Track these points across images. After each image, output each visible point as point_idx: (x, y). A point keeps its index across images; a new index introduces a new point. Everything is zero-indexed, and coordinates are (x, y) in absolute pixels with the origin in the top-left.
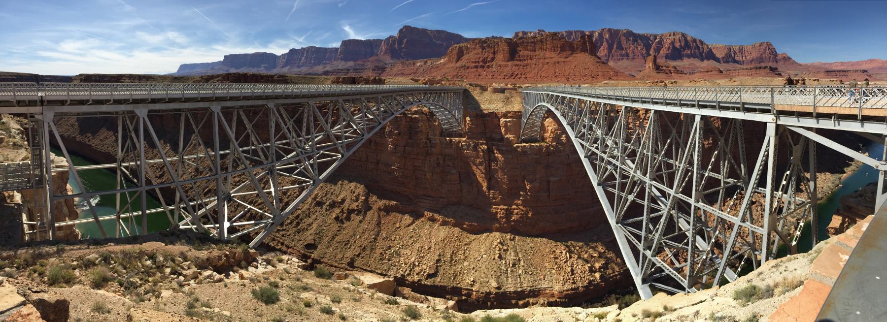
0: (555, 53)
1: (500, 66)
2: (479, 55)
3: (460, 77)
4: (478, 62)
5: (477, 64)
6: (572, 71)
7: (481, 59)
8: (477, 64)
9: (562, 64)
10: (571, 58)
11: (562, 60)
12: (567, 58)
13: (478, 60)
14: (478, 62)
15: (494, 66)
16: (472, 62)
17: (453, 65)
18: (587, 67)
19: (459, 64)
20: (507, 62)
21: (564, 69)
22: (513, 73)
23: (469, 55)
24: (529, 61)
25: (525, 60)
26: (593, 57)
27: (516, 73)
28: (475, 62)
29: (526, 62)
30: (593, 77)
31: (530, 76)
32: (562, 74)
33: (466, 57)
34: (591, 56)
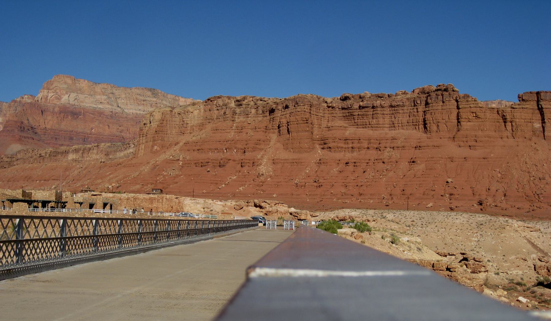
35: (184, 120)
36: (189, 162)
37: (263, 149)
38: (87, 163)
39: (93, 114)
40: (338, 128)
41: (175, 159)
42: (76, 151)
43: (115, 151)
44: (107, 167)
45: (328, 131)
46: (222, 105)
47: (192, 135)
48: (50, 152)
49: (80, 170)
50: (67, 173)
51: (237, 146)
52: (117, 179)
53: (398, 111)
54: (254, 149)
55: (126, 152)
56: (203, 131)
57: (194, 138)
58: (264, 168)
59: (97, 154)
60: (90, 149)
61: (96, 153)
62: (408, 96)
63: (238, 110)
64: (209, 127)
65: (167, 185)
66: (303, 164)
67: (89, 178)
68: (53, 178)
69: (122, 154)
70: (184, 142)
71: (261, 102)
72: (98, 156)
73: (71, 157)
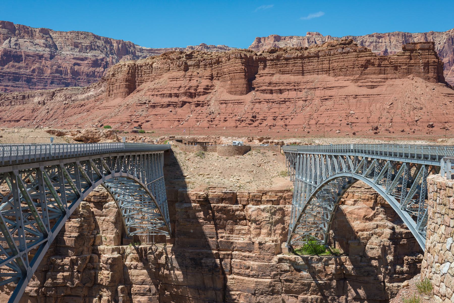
0: (347, 78)
1: (225, 102)
2: (179, 83)
3: (136, 125)
4: (177, 95)
5: (174, 99)
6: (385, 113)
7: (182, 90)
8: (174, 99)
9: (364, 100)
10: (384, 88)
11: (365, 91)
12: (373, 87)
13: (176, 91)
14: (177, 95)
15: (212, 103)
16: (163, 95)
17: (118, 100)
18: (419, 106)
19: (133, 98)
20: (242, 94)
21: (367, 111)
22: (254, 117)
23: (157, 81)
24: (292, 94)
25: (281, 91)
26: (431, 85)
27: (260, 117)
28: (170, 95)
29: (285, 95)
30: (432, 126)
31: (294, 122)
32: (365, 120)
33: (145, 86)
34: (429, 84)
35: (145, 71)
36: (154, 104)
37: (210, 93)
38: (52, 105)
39: (33, 57)
40: (267, 75)
41: (142, 103)
42: (42, 95)
43: (76, 95)
44: (71, 108)
45: (260, 77)
46: (175, 58)
47: (153, 82)
48: (17, 97)
49: (47, 111)
50: (36, 113)
51: (191, 91)
52: (98, 119)
53: (312, 61)
54: (205, 93)
55: (86, 95)
56: (162, 79)
57: (155, 86)
58: (214, 107)
59: (60, 97)
60: (54, 93)
61: (59, 96)
62: (319, 49)
63: (189, 63)
64: (166, 76)
65: (141, 123)
66: (242, 103)
67: (56, 117)
68: (23, 118)
69: (84, 96)
70: (147, 88)
71: (206, 55)
72: (62, 98)
73: (36, 100)
